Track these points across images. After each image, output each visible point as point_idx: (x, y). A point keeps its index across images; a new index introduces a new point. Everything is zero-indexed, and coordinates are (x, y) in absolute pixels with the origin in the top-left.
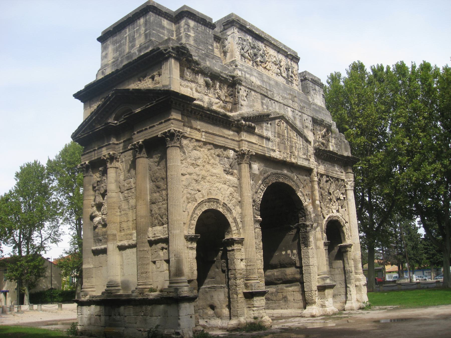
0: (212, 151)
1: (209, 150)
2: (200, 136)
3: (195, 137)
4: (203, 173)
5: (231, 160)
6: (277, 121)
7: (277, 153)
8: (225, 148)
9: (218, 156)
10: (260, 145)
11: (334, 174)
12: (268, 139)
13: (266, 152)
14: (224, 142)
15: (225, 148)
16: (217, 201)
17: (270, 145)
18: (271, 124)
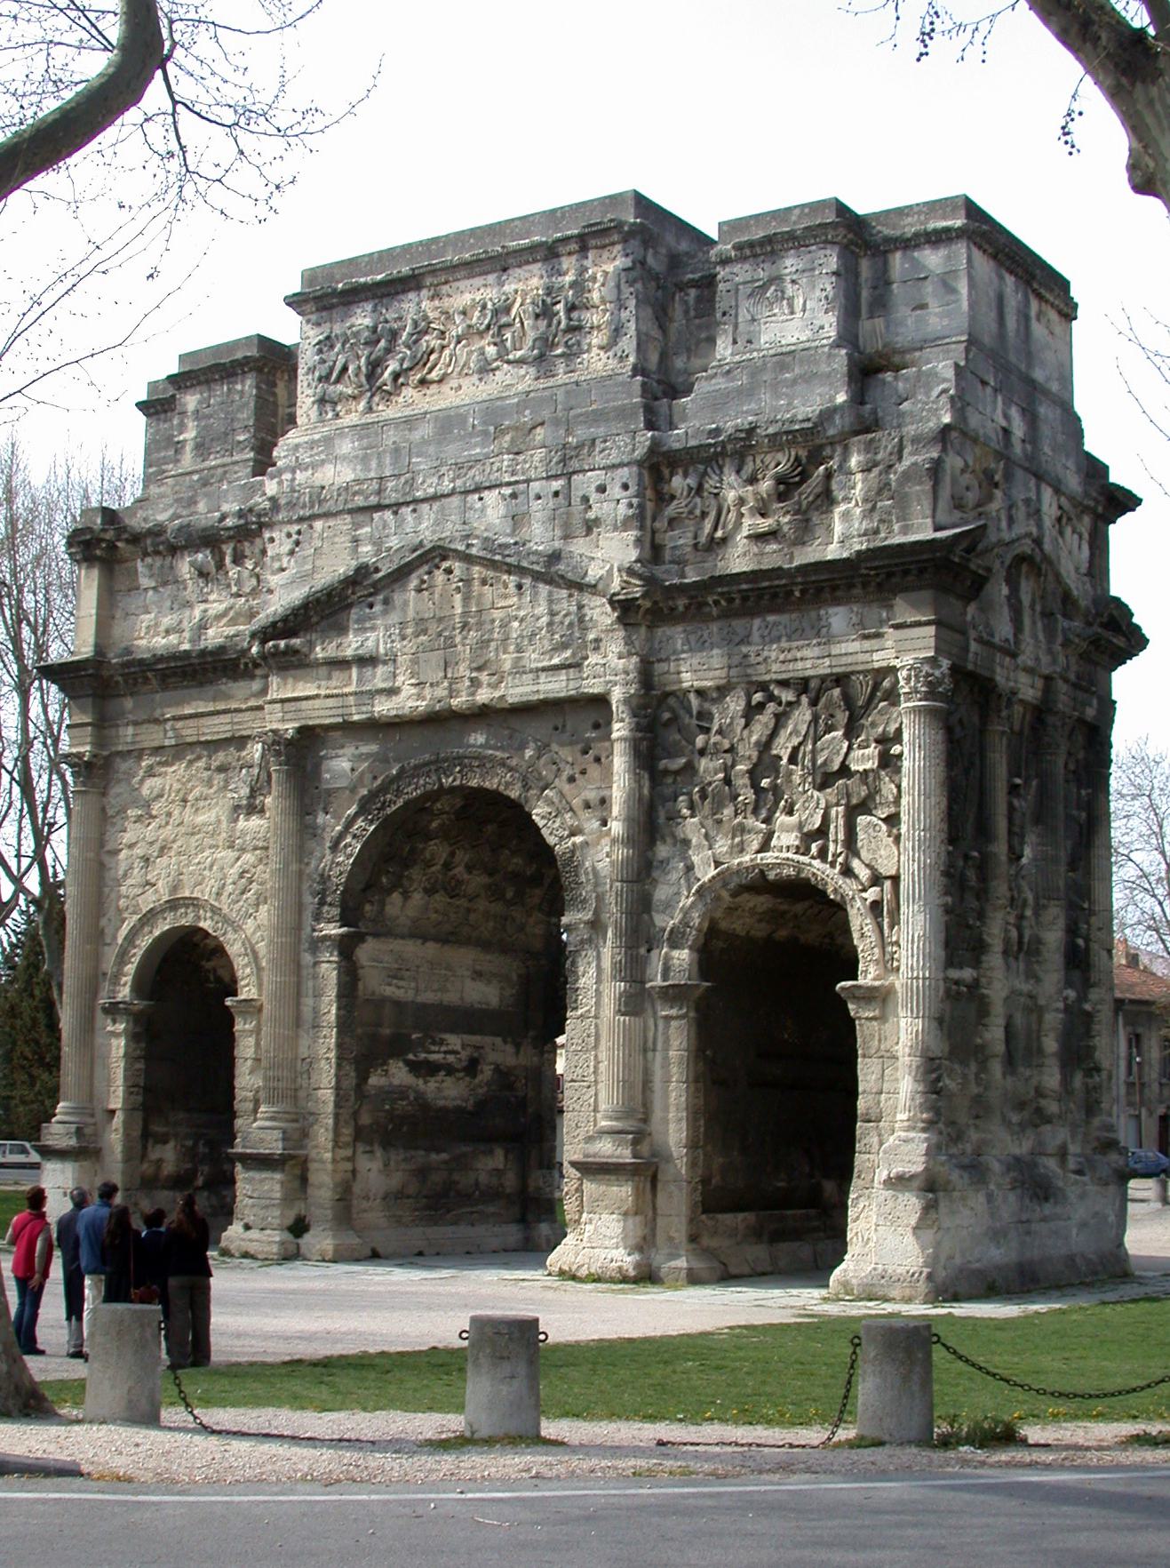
0: (201, 764)
1: (191, 762)
2: (161, 735)
3: (146, 745)
4: (167, 832)
5: (256, 771)
6: (414, 582)
7: (408, 690)
8: (240, 741)
9: (222, 769)
10: (327, 696)
11: (800, 665)
12: (367, 661)
13: (354, 710)
14: (228, 727)
15: (240, 741)
16: (193, 903)
17: (379, 677)
18: (386, 602)
